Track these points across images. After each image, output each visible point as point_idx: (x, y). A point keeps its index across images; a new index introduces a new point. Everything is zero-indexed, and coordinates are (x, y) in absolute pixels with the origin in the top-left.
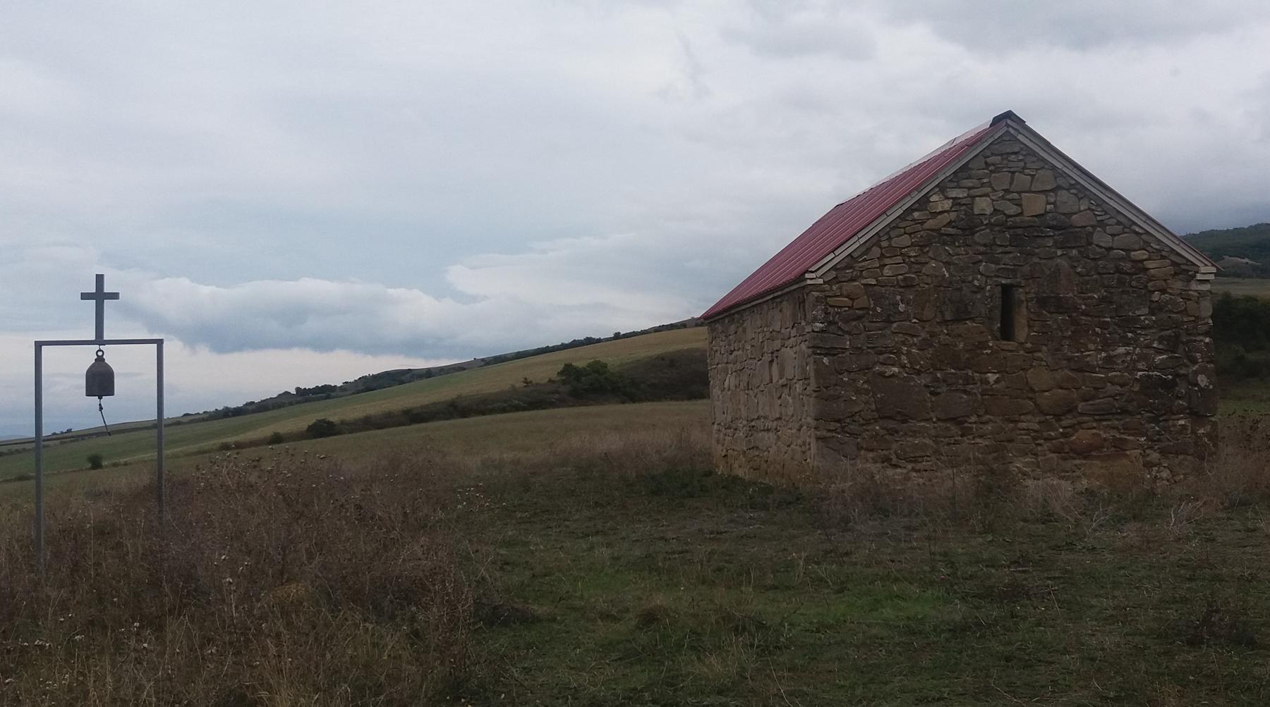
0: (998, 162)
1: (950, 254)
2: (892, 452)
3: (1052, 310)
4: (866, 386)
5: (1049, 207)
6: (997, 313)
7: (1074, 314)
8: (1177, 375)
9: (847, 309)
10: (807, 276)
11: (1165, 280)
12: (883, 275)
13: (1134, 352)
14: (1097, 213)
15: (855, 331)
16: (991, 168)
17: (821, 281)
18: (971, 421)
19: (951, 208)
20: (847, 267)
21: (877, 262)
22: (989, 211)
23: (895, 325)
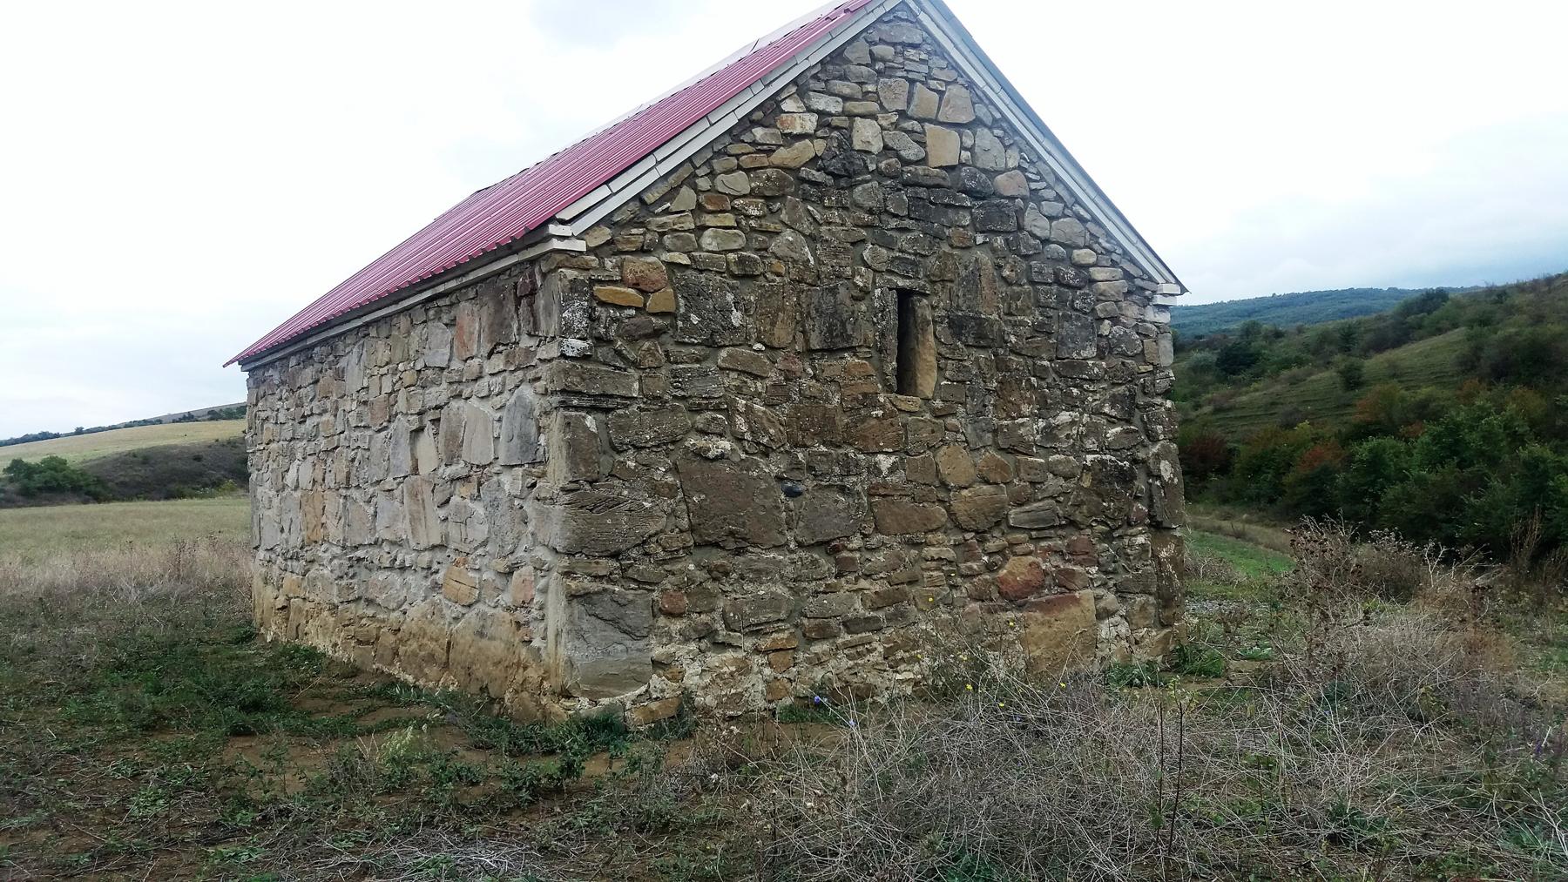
0: (890, 57)
1: (815, 219)
2: (716, 615)
3: (971, 341)
4: (670, 479)
5: (966, 155)
6: (892, 341)
7: (1001, 351)
8: (1135, 461)
9: (634, 312)
10: (553, 229)
11: (1116, 302)
12: (700, 248)
13: (1081, 420)
14: (1030, 176)
15: (649, 362)
16: (879, 66)
17: (580, 246)
18: (850, 546)
19: (815, 131)
20: (635, 222)
21: (691, 219)
22: (876, 147)
23: (724, 353)
